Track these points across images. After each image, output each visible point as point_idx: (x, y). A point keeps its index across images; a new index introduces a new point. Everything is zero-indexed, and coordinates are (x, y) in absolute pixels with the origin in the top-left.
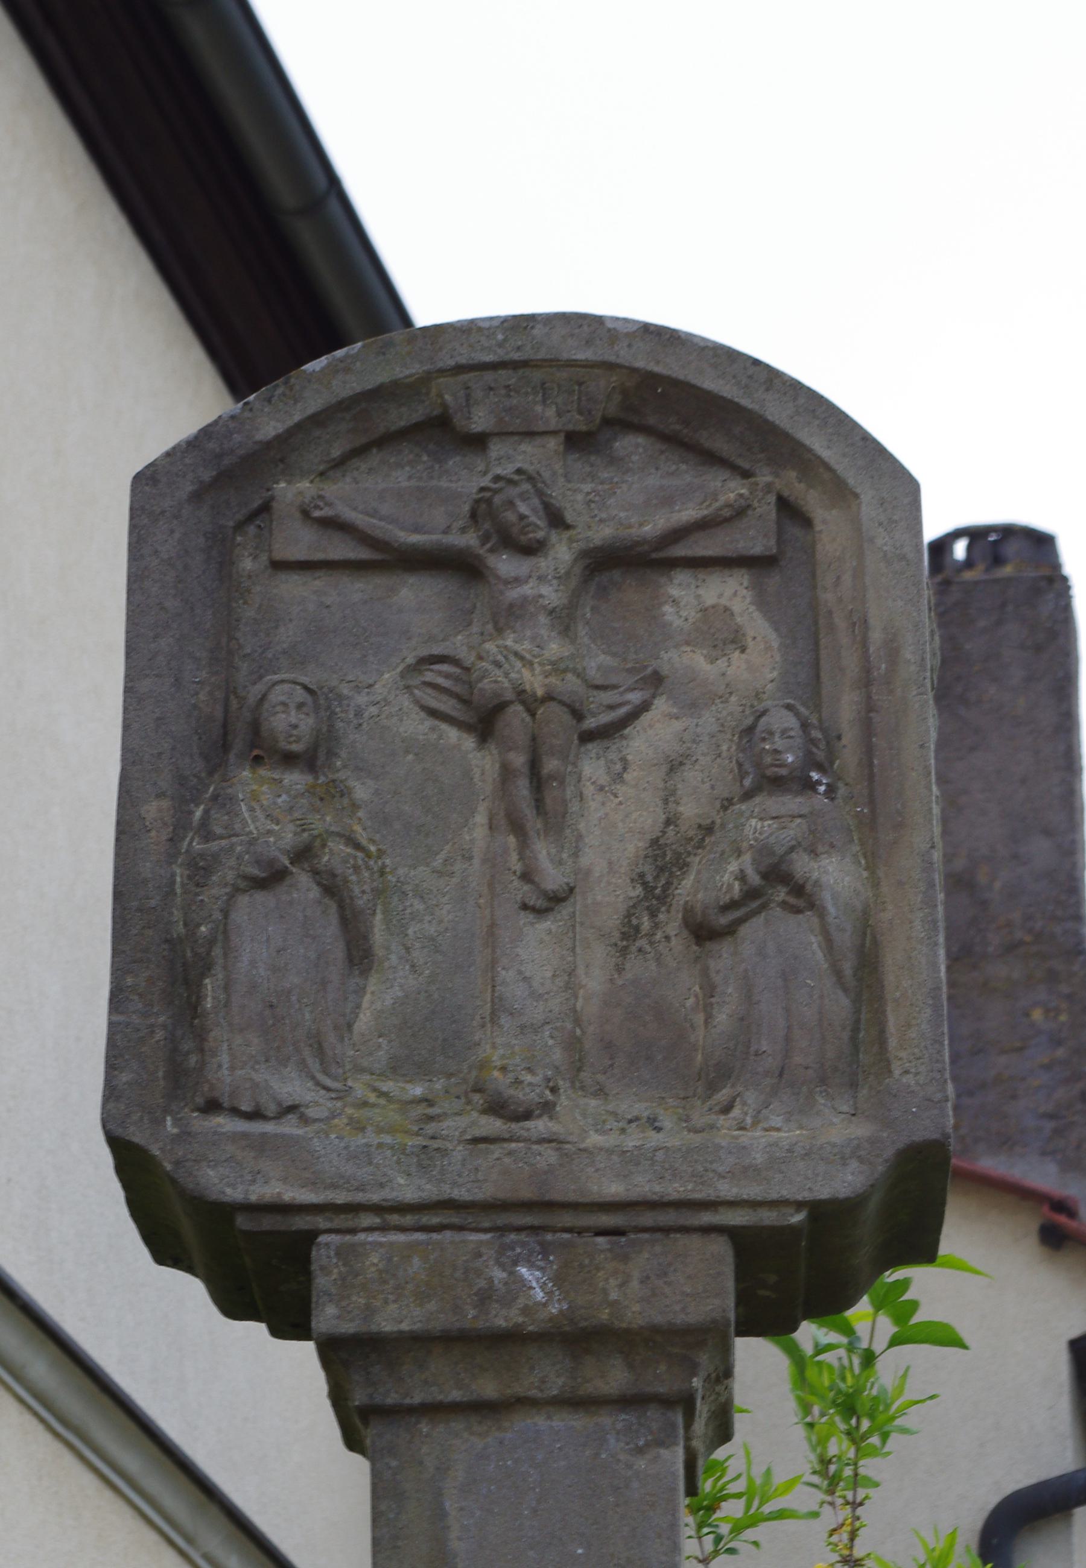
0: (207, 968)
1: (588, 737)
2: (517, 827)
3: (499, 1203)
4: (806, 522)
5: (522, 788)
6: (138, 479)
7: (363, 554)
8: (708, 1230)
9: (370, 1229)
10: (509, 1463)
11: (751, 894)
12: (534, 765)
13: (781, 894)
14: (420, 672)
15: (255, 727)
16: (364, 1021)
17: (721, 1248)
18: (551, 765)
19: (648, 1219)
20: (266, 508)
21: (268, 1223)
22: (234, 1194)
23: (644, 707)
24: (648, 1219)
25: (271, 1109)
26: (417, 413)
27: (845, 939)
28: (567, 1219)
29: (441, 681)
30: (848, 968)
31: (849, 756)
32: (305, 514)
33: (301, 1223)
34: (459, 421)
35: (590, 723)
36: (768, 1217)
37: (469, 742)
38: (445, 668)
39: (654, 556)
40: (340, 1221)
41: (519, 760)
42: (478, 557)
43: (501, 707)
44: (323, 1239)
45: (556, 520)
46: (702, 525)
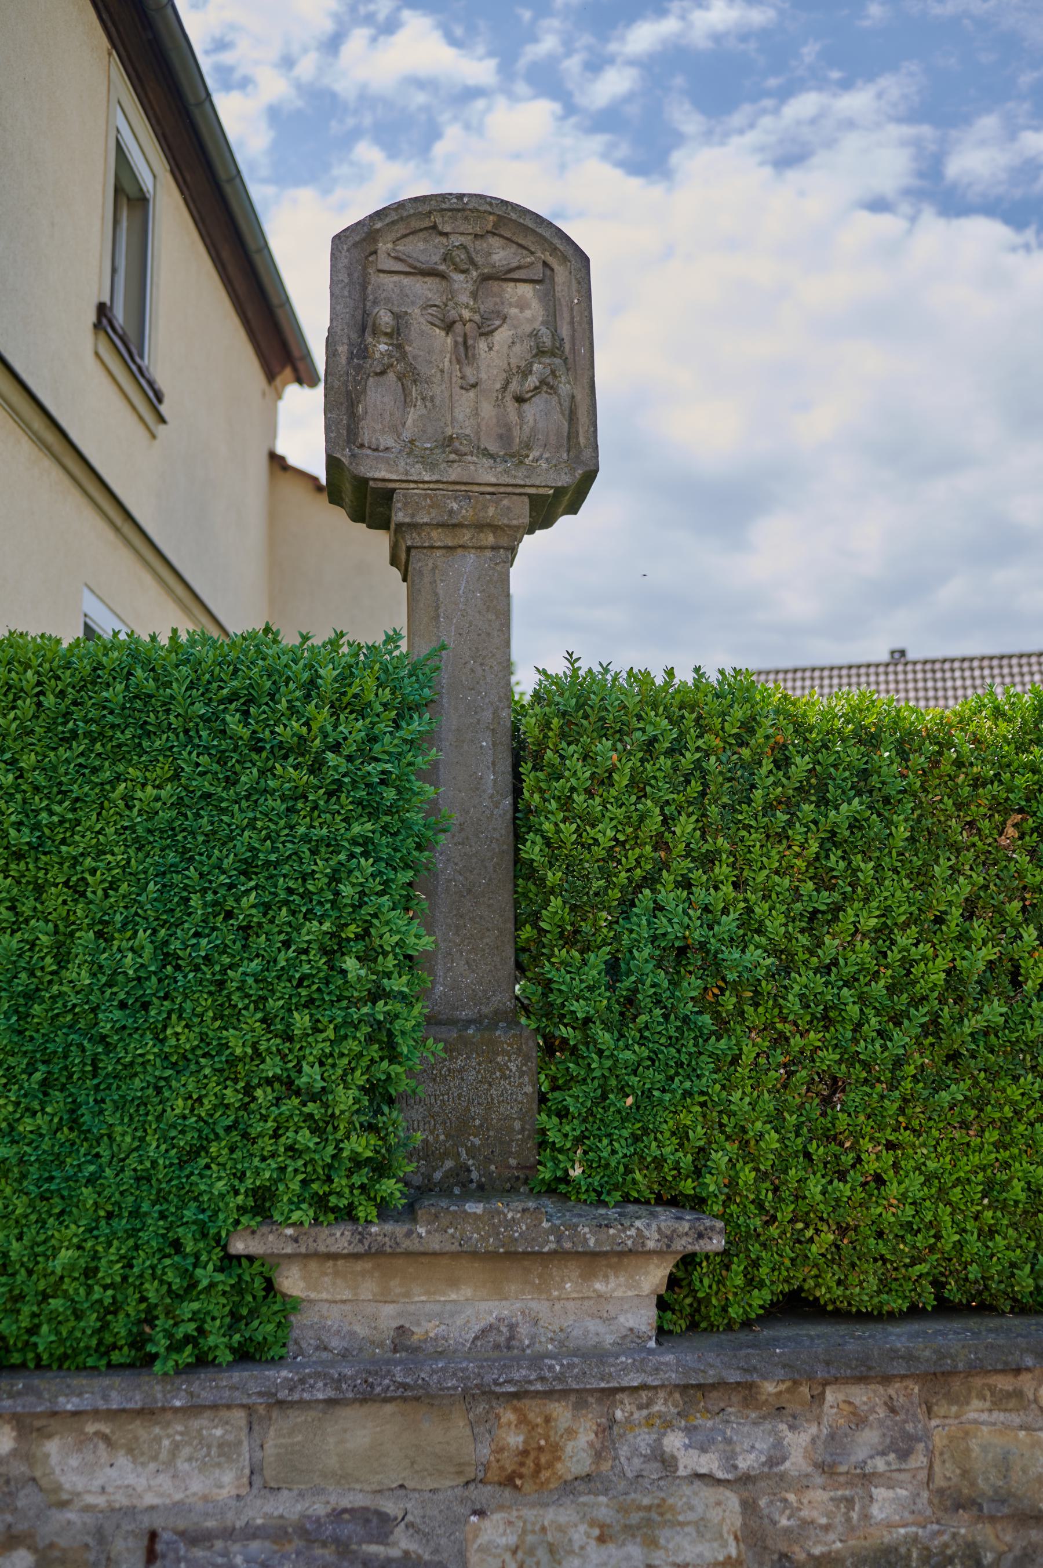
0: (359, 402)
1: (481, 335)
2: (459, 362)
4: (552, 270)
5: (462, 349)
6: (334, 238)
7: (408, 269)
8: (520, 494)
11: (536, 388)
12: (465, 343)
13: (545, 388)
15: (374, 324)
16: (409, 422)
17: (526, 500)
18: (470, 342)
19: (502, 489)
20: (375, 252)
21: (380, 485)
22: (369, 475)
23: (499, 326)
24: (502, 489)
25: (382, 447)
26: (427, 224)
27: (566, 404)
28: (476, 488)
30: (567, 412)
31: (567, 346)
34: (440, 227)
35: (483, 330)
36: (541, 491)
37: (443, 333)
40: (404, 485)
41: (460, 339)
43: (454, 322)
45: (472, 262)
46: (519, 268)
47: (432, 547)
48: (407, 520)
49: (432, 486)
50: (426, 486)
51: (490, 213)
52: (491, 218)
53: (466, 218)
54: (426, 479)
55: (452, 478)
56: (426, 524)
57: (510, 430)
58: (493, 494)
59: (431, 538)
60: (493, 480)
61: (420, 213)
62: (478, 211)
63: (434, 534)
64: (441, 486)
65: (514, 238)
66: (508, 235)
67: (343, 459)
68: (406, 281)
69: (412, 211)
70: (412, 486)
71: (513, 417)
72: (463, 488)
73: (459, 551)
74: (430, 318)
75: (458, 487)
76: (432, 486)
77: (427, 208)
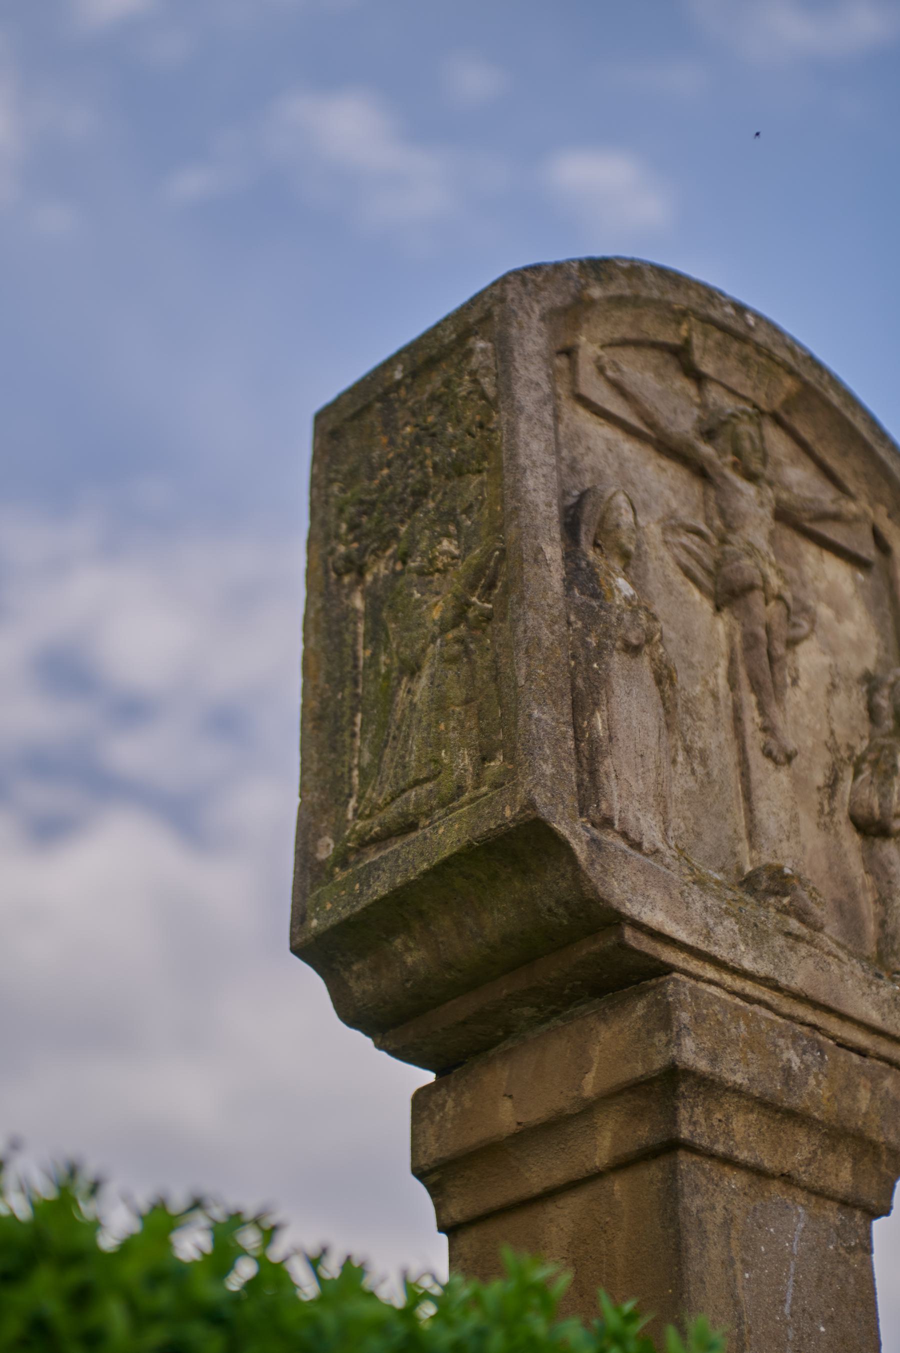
3: (803, 995)
9: (710, 982)
10: (772, 1230)
14: (679, 534)
22: (633, 909)
26: (668, 336)
29: (695, 548)
32: (601, 370)
33: (669, 956)
34: (697, 356)
37: (707, 606)
38: (696, 539)
39: (807, 525)
40: (694, 966)
42: (711, 464)
43: (751, 587)
44: (675, 975)
47: (728, 1161)
48: (703, 1065)
49: (749, 988)
50: (739, 984)
51: (791, 372)
52: (789, 383)
53: (744, 361)
54: (747, 964)
55: (798, 982)
56: (737, 1091)
57: (853, 896)
58: (862, 1052)
59: (729, 1134)
60: (875, 1017)
61: (668, 306)
62: (770, 356)
63: (738, 1124)
64: (766, 995)
65: (819, 449)
66: (807, 434)
67: (574, 844)
68: (628, 447)
69: (656, 294)
70: (710, 972)
71: (855, 866)
72: (811, 1016)
73: (776, 1187)
74: (684, 558)
75: (801, 1011)
76: (749, 988)
77: (679, 300)
